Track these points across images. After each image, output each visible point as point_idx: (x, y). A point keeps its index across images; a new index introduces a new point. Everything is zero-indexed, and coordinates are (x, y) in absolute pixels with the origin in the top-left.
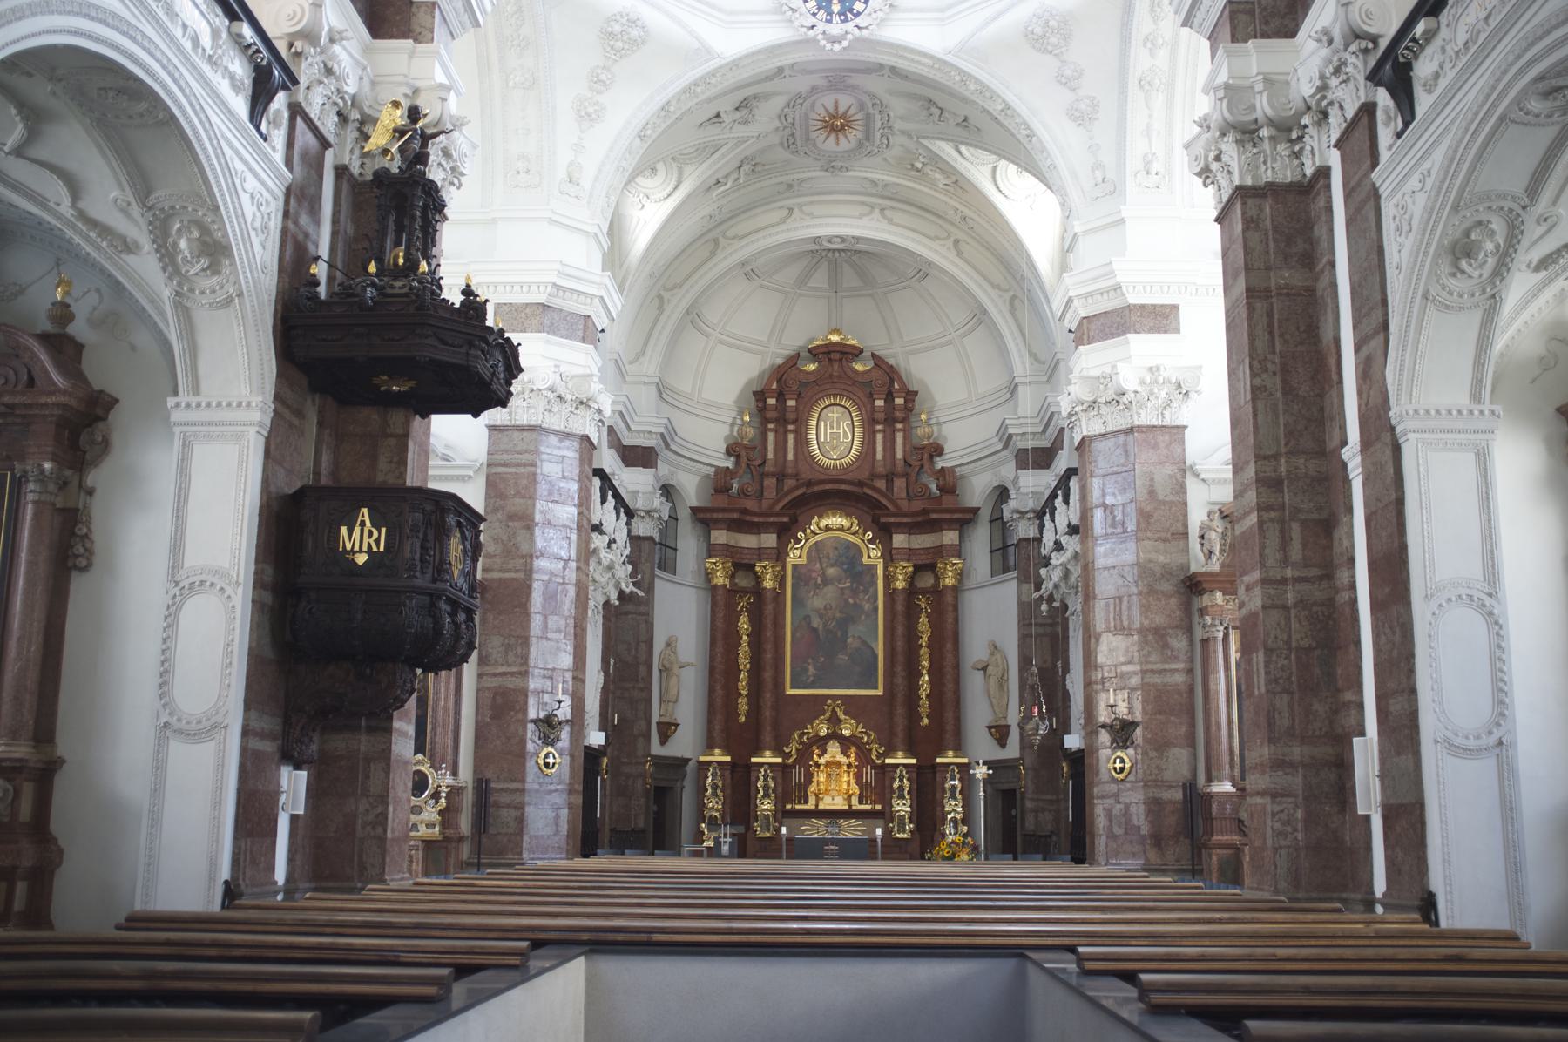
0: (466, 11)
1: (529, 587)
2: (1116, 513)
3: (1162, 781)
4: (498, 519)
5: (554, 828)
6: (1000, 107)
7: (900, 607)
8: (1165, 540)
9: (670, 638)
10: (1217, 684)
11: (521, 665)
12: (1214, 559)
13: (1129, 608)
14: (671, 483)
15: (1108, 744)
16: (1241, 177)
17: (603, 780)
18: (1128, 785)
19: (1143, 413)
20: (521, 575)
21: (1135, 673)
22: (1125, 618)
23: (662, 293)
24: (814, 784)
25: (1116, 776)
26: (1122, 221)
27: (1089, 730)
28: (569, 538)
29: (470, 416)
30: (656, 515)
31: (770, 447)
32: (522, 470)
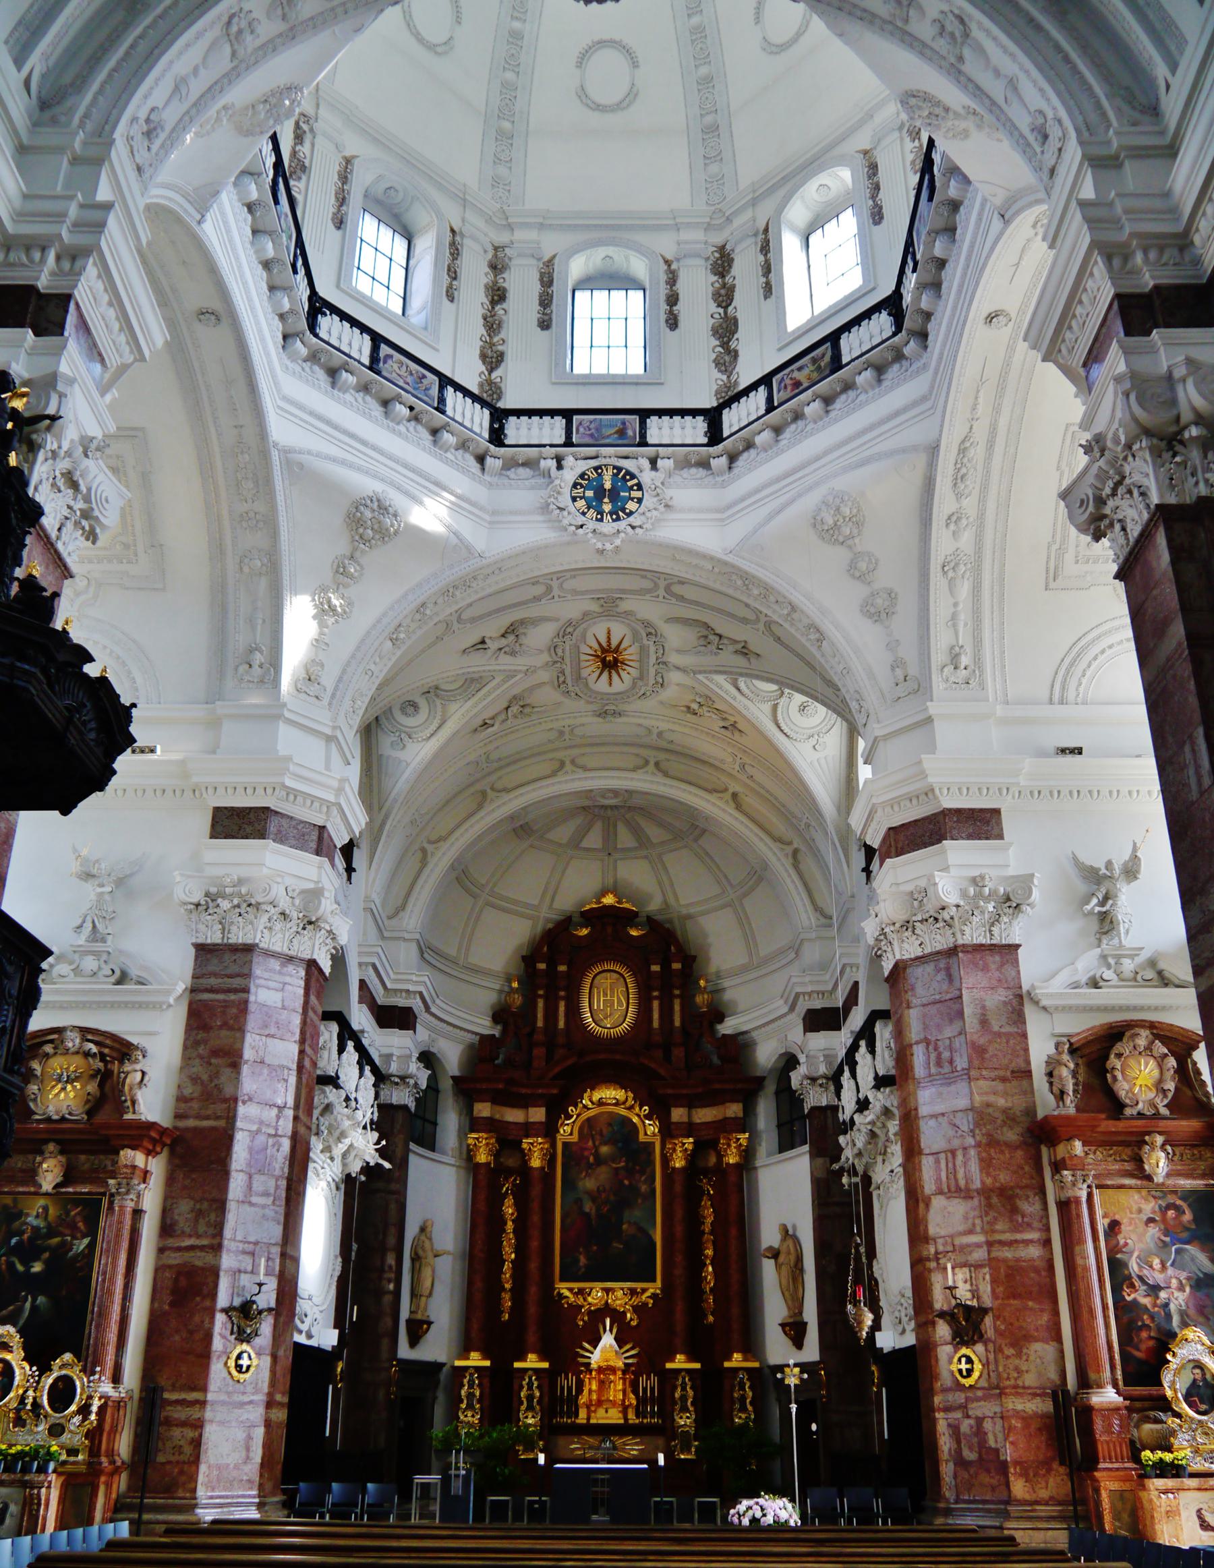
0: (106, 290)
1: (231, 1138)
2: (941, 1049)
3: (1024, 1387)
5: (244, 1454)
6: (785, 612)
7: (678, 1188)
8: (1004, 1080)
9: (425, 1222)
10: (1085, 1258)
11: (214, 1236)
12: (1068, 1100)
13: (965, 1164)
14: (432, 1050)
15: (948, 1337)
16: (1161, 496)
17: (335, 1389)
18: (979, 1393)
19: (967, 930)
20: (221, 1123)
21: (978, 1245)
22: (960, 1175)
23: (426, 845)
24: (586, 1392)
25: (963, 1381)
26: (929, 720)
27: (922, 1319)
28: (286, 1081)
29: (56, 814)
30: (412, 1082)
31: (540, 1015)
32: (232, 997)
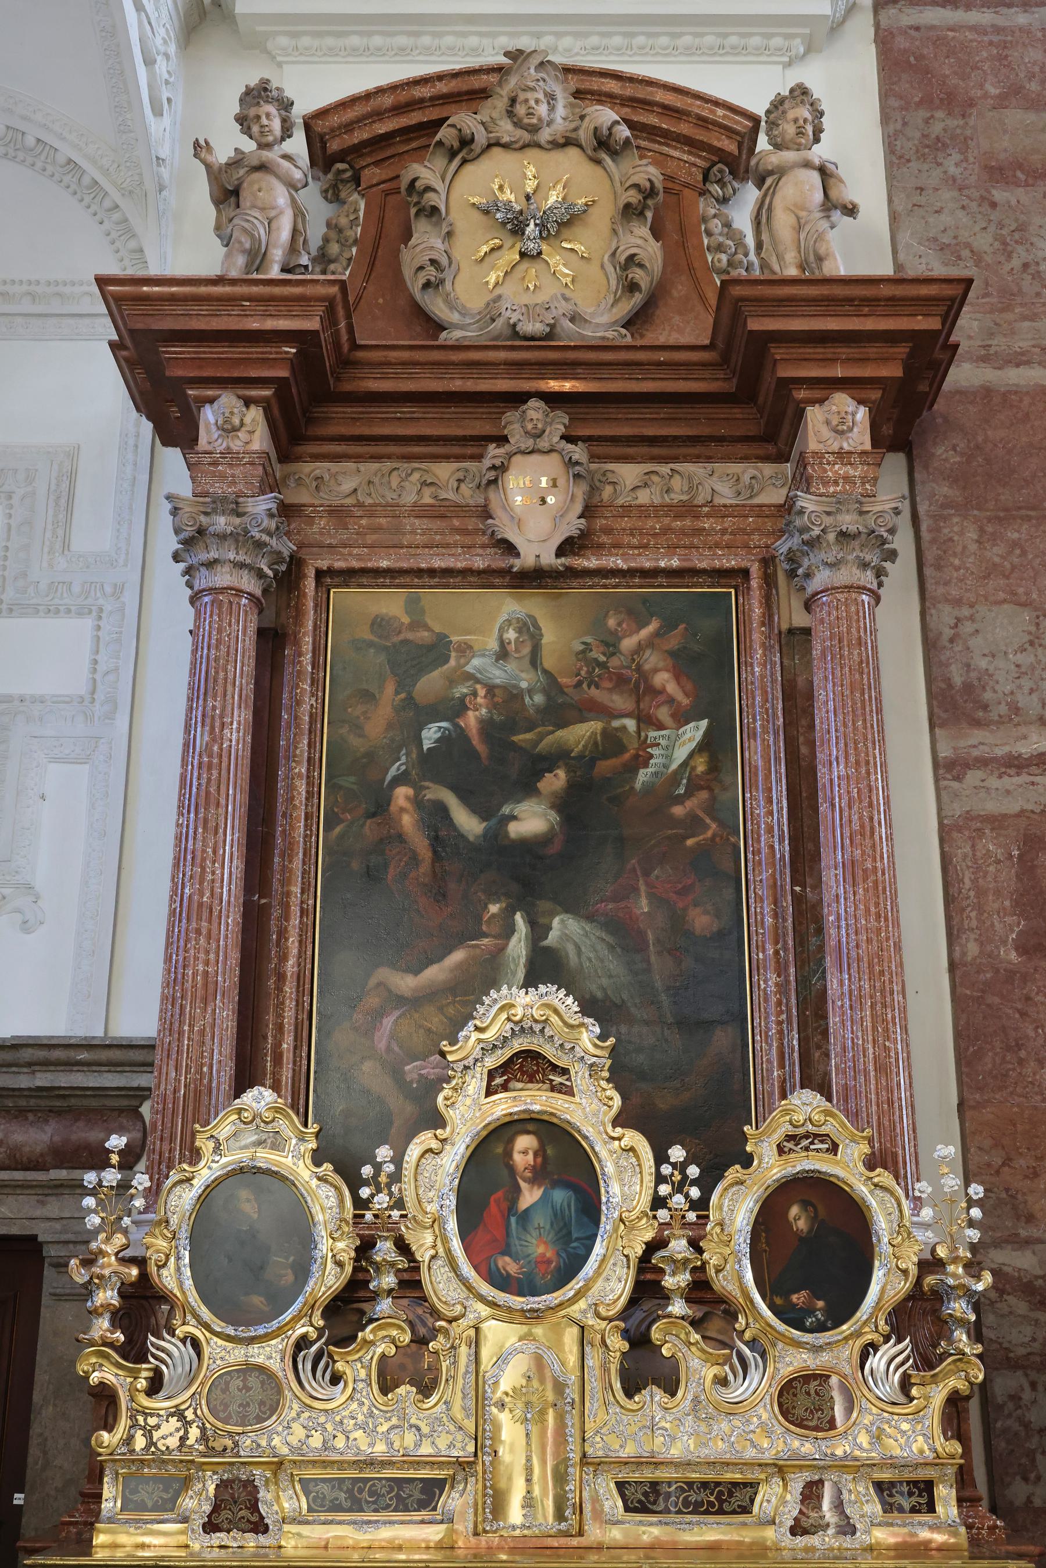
4: (951, 181)
